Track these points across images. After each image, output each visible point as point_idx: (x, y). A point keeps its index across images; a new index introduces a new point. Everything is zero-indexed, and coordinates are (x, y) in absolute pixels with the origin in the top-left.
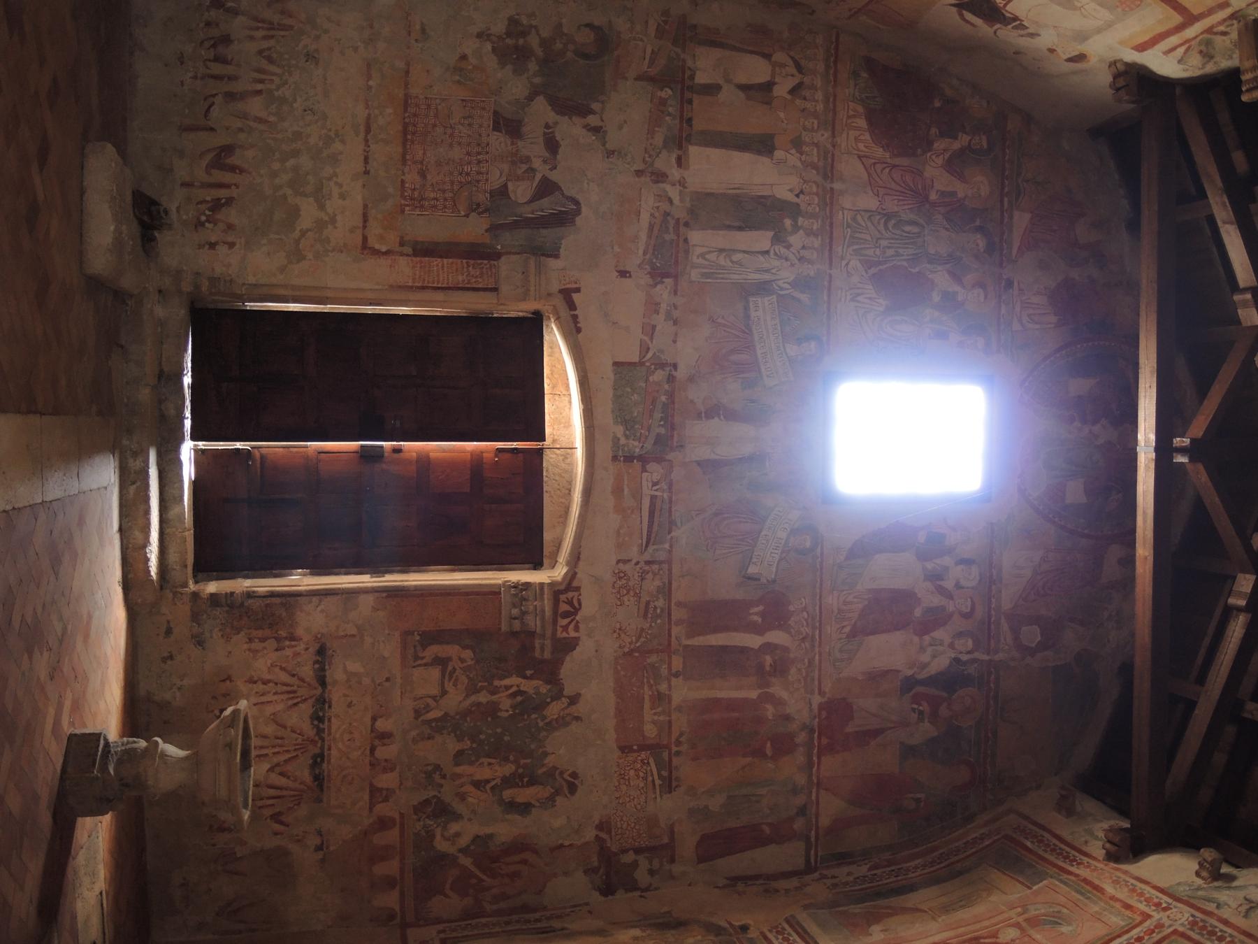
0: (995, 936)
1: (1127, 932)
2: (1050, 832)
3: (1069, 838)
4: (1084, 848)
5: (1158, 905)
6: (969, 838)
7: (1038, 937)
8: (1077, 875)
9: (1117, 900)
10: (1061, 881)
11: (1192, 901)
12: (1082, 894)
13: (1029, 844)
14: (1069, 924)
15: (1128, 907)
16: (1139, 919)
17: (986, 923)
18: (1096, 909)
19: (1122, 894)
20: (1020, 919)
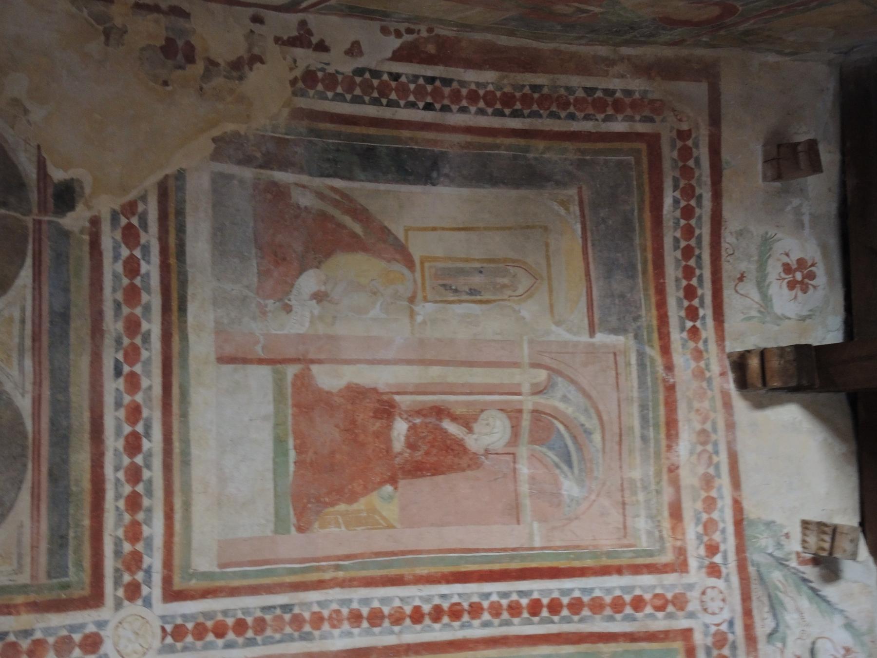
0: (467, 423)
1: (636, 570)
2: (717, 196)
3: (728, 239)
4: (728, 293)
5: (712, 549)
6: (602, 83)
7: (524, 469)
8: (669, 368)
9: (675, 483)
10: (641, 355)
11: (757, 591)
12: (644, 419)
13: (668, 201)
14: (580, 482)
15: (676, 513)
16: (668, 557)
17: (479, 376)
18: (636, 474)
19: (688, 478)
20: (528, 403)
